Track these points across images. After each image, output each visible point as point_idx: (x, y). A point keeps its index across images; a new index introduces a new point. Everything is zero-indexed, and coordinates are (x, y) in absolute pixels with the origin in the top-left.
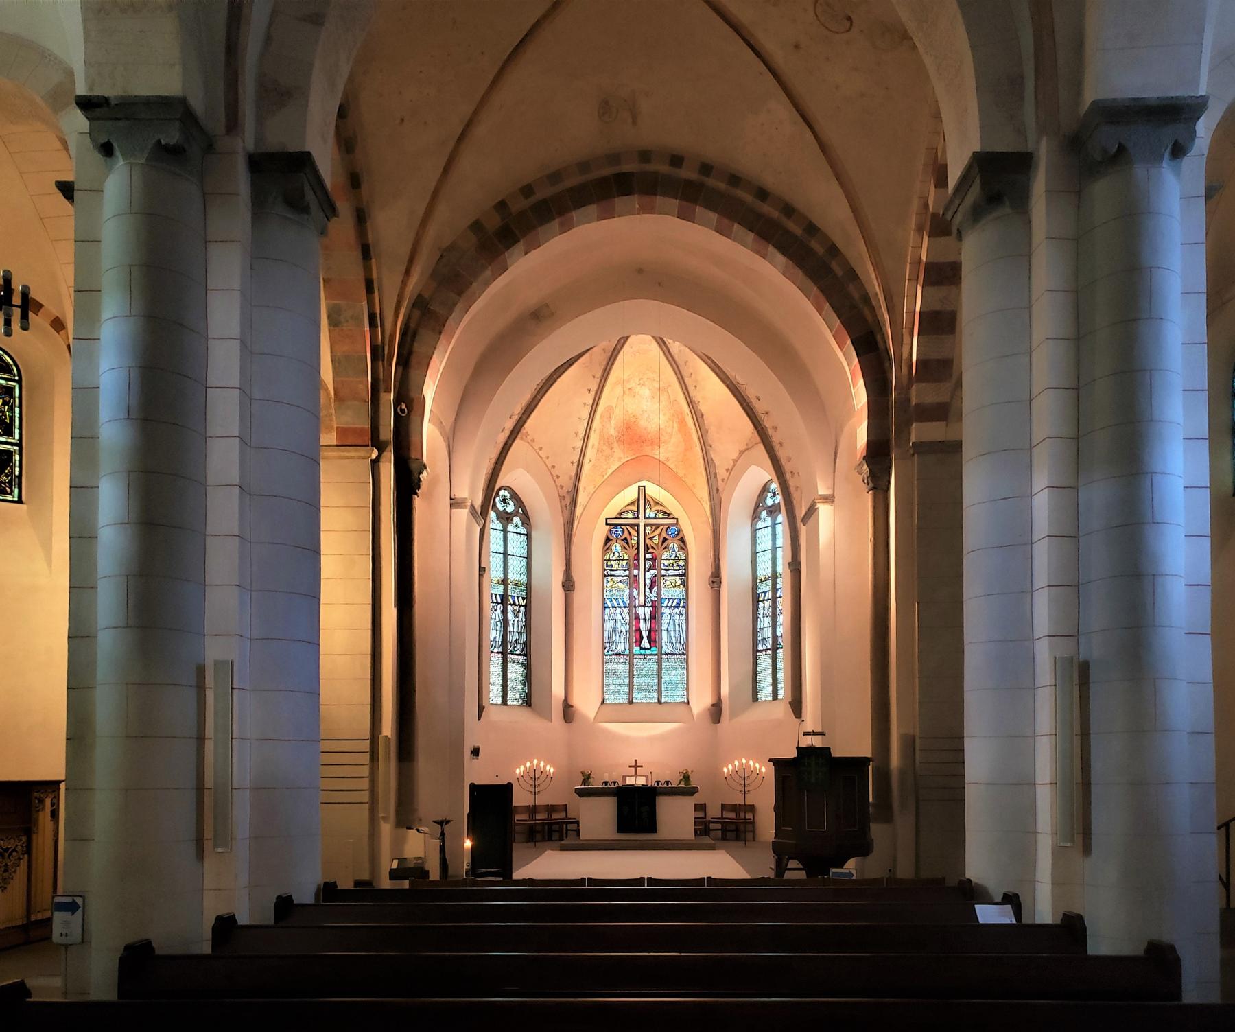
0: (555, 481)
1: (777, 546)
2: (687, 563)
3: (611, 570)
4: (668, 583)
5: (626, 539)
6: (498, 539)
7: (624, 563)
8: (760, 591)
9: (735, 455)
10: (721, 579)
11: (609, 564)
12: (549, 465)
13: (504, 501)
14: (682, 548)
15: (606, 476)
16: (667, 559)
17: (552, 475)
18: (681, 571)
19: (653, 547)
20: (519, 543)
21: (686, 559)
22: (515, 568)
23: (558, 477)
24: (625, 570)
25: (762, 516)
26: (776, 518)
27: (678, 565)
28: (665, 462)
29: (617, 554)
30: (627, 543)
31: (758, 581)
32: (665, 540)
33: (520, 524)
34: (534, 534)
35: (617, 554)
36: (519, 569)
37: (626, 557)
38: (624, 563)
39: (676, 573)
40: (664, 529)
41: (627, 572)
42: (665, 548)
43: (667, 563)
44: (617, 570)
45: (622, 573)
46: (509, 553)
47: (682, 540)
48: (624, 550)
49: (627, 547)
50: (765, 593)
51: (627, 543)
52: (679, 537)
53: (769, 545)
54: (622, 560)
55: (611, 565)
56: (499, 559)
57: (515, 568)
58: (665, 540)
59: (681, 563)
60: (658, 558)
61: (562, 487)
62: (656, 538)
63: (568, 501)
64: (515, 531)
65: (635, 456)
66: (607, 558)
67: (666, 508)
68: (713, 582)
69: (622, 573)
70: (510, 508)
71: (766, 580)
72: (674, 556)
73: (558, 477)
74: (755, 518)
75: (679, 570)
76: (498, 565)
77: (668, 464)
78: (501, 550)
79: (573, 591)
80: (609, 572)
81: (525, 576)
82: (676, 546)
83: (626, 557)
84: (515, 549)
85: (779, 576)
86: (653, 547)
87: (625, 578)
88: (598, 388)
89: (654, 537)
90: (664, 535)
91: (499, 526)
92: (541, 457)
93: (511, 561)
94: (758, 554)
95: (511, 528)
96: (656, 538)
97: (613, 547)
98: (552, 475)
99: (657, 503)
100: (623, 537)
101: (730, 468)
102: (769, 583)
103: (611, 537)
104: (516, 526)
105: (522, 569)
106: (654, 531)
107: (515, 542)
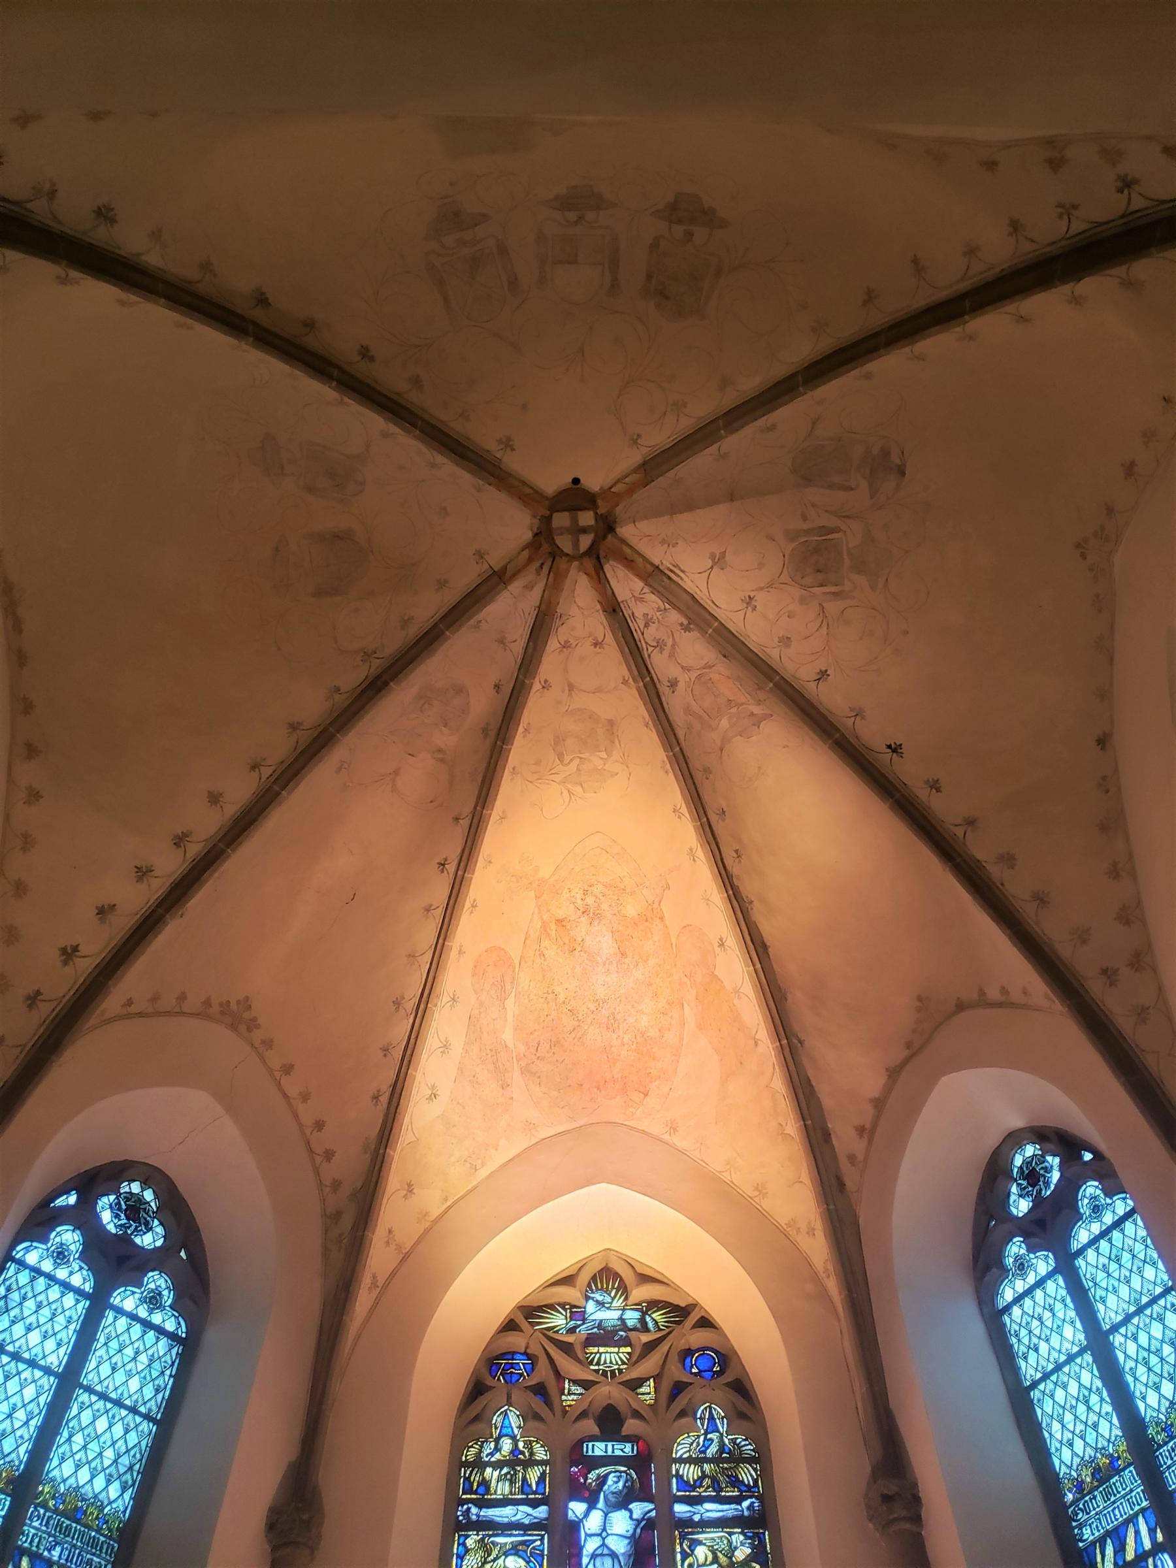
0: (317, 1171)
1: (1106, 1327)
2: (766, 1474)
3: (482, 1504)
4: (701, 1552)
5: (540, 1390)
6: (61, 1320)
7: (533, 1475)
8: (1088, 1534)
9: (873, 1084)
10: (915, 1485)
11: (476, 1479)
12: (307, 1119)
13: (134, 1210)
14: (743, 1416)
15: (483, 1173)
16: (690, 1461)
17: (310, 1150)
18: (746, 1504)
19: (637, 1414)
20: (143, 1358)
21: (761, 1459)
22: (94, 1447)
23: (329, 1155)
24: (534, 1504)
25: (1009, 1261)
26: (1067, 1236)
27: (735, 1482)
28: (666, 1137)
29: (507, 1445)
30: (548, 1402)
31: (1070, 1497)
32: (678, 1388)
33: (168, 1298)
34: (212, 1336)
35: (507, 1445)
36: (109, 1454)
37: (541, 1453)
38: (533, 1475)
39: (729, 1510)
40: (674, 1356)
41: (542, 1512)
42: (682, 1414)
43: (691, 1472)
44: (504, 1502)
45: (523, 1514)
46: (89, 1377)
47: (742, 1389)
48: (533, 1424)
49: (543, 1410)
50: (1117, 1535)
51: (548, 1402)
52: (728, 1377)
53: (1073, 1335)
54: (530, 1463)
55: (485, 1484)
56: (29, 1392)
57: (94, 1447)
58: (678, 1388)
59: (747, 1474)
60: (657, 1452)
61: (336, 1185)
62: (648, 1388)
63: (347, 1223)
64: (143, 1313)
65: (575, 1125)
66: (471, 1458)
67: (677, 1288)
68: (887, 1499)
69: (523, 1514)
70: (150, 1240)
71: (1104, 1473)
72: (712, 1450)
73: (329, 1155)
74: (987, 1268)
75: (738, 1500)
76: (21, 1415)
77: (676, 1140)
78: (56, 1358)
79: (312, 1550)
80: (474, 1510)
81: (127, 1496)
82: (718, 1411)
83: (541, 1453)
84: (120, 1377)
85: (1160, 1438)
86: (637, 1414)
87: (532, 1536)
88: (463, 850)
89: (640, 1382)
90: (676, 1372)
91: (81, 1278)
92: (285, 1095)
93: (86, 1417)
94: (1035, 1394)
95: (127, 1299)
96: (648, 1388)
97: (497, 1419)
98: (310, 1150)
99: (645, 1279)
100: (532, 1382)
101: (868, 1126)
102: (1130, 1481)
103: (489, 1381)
104: (153, 1300)
105: (125, 1461)
106: (637, 1362)
107: (129, 1352)
